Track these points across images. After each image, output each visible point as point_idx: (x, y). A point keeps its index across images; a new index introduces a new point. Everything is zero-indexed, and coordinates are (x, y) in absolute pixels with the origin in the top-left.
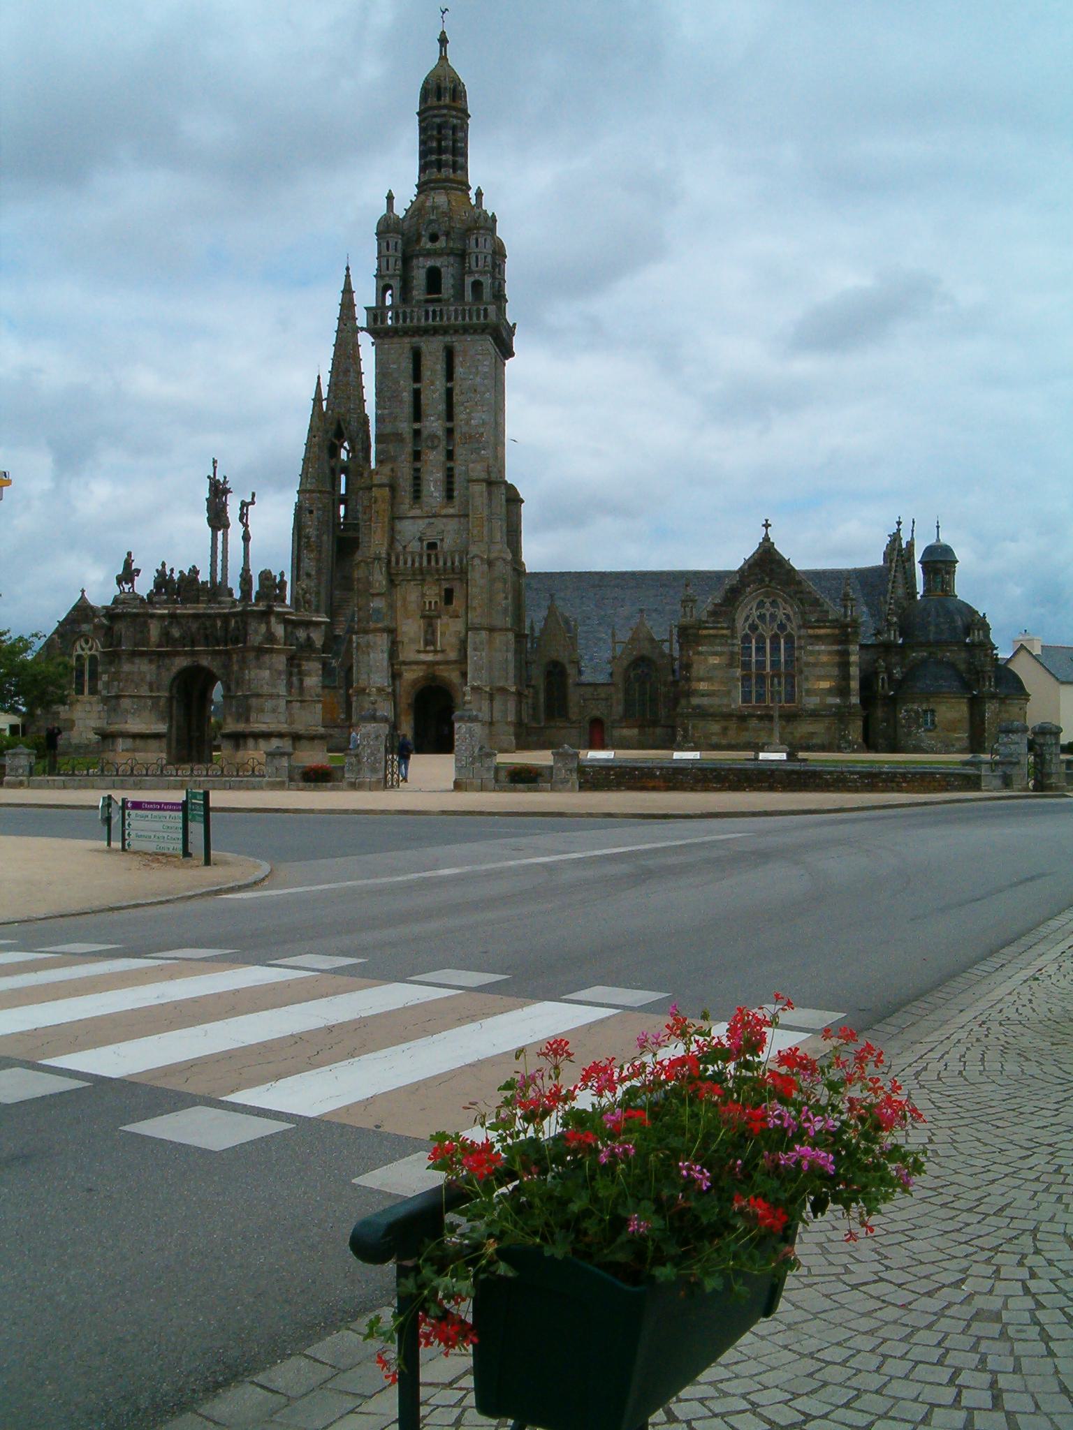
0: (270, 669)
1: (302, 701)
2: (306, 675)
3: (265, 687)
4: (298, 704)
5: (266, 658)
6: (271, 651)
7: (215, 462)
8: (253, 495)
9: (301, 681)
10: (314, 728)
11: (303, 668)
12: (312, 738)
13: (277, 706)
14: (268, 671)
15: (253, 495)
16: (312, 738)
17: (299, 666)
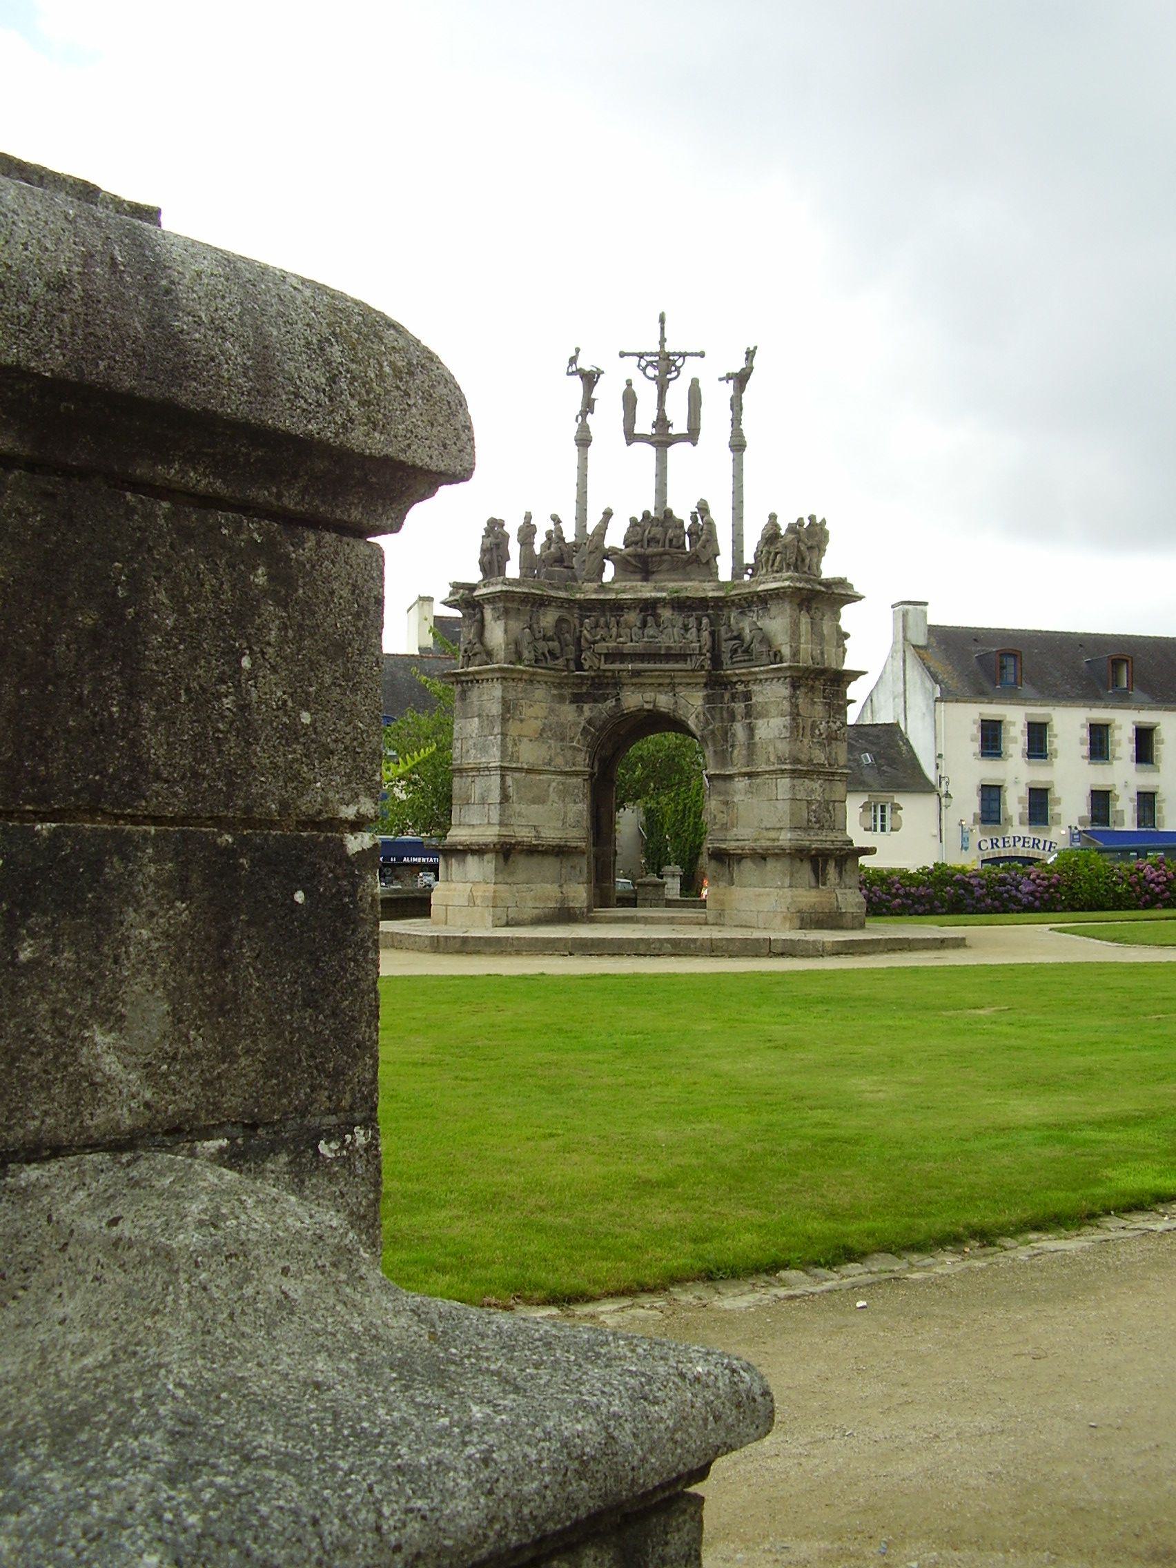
0: (479, 716)
1: (750, 775)
2: (760, 716)
3: (473, 752)
4: (746, 781)
5: (474, 694)
6: (474, 680)
7: (662, 320)
8: (750, 354)
9: (751, 729)
10: (772, 834)
11: (754, 700)
12: (761, 857)
13: (489, 790)
14: (476, 719)
15: (750, 354)
16: (761, 857)
17: (747, 696)
